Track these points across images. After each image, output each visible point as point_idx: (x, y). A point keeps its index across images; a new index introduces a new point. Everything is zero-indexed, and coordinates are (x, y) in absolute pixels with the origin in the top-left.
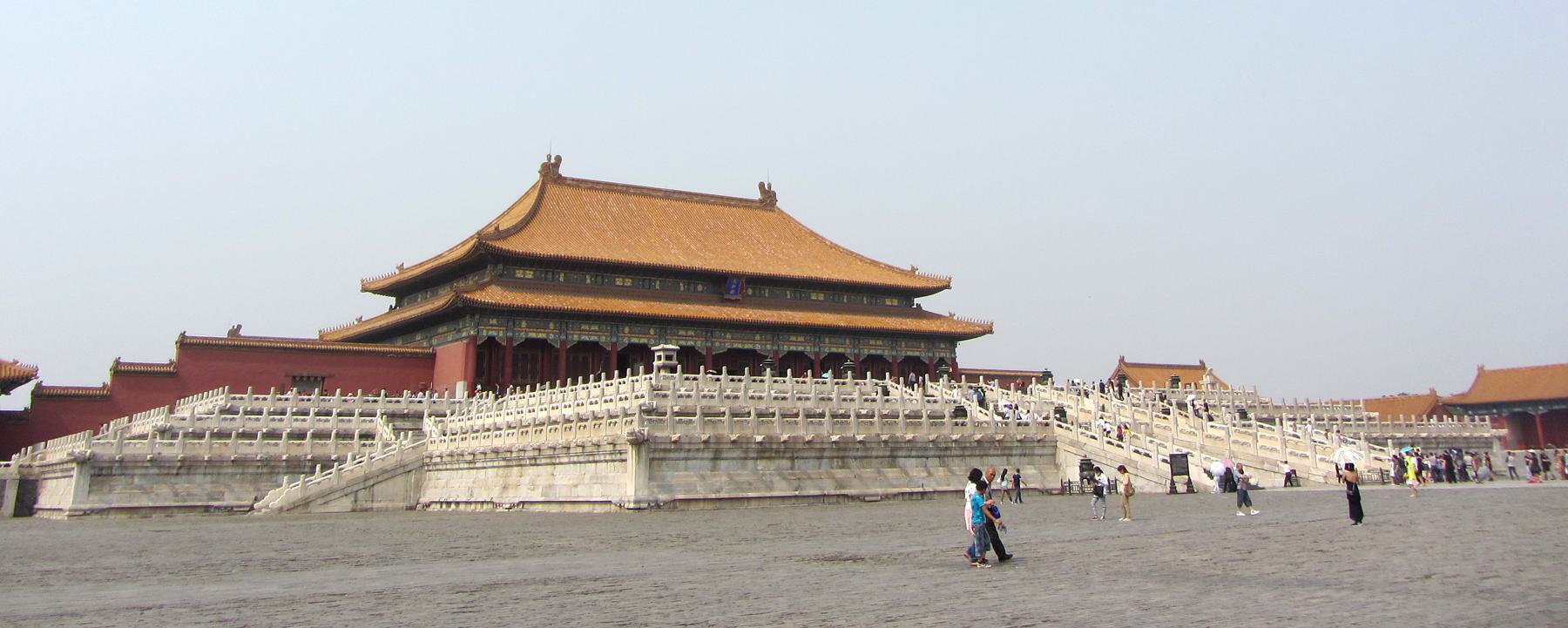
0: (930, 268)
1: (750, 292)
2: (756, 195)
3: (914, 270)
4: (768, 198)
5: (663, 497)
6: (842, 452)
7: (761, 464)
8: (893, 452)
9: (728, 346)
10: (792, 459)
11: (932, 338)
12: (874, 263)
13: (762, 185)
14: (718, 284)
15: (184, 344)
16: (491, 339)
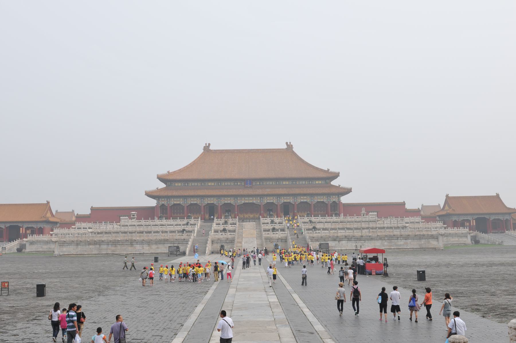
0: (333, 169)
1: (258, 183)
2: (285, 147)
3: (328, 170)
4: (290, 147)
5: (61, 254)
6: (115, 243)
7: (91, 246)
8: (132, 243)
9: (243, 202)
10: (100, 245)
11: (328, 195)
12: (317, 169)
13: (287, 143)
14: (248, 182)
15: (92, 209)
16: (163, 204)
